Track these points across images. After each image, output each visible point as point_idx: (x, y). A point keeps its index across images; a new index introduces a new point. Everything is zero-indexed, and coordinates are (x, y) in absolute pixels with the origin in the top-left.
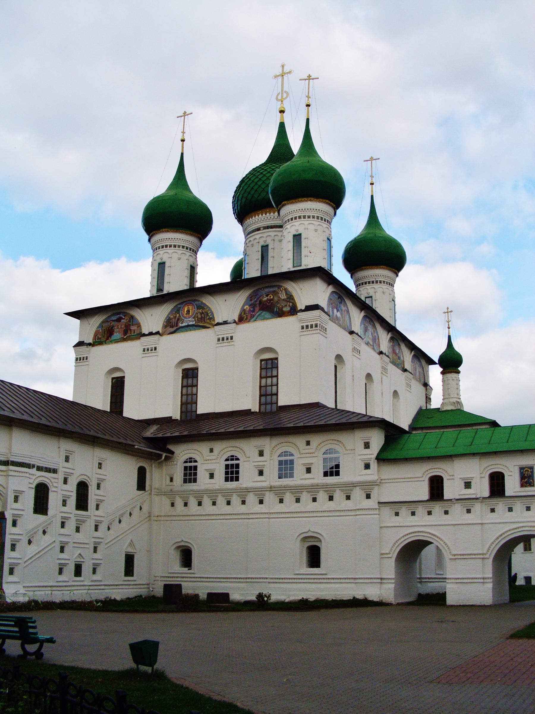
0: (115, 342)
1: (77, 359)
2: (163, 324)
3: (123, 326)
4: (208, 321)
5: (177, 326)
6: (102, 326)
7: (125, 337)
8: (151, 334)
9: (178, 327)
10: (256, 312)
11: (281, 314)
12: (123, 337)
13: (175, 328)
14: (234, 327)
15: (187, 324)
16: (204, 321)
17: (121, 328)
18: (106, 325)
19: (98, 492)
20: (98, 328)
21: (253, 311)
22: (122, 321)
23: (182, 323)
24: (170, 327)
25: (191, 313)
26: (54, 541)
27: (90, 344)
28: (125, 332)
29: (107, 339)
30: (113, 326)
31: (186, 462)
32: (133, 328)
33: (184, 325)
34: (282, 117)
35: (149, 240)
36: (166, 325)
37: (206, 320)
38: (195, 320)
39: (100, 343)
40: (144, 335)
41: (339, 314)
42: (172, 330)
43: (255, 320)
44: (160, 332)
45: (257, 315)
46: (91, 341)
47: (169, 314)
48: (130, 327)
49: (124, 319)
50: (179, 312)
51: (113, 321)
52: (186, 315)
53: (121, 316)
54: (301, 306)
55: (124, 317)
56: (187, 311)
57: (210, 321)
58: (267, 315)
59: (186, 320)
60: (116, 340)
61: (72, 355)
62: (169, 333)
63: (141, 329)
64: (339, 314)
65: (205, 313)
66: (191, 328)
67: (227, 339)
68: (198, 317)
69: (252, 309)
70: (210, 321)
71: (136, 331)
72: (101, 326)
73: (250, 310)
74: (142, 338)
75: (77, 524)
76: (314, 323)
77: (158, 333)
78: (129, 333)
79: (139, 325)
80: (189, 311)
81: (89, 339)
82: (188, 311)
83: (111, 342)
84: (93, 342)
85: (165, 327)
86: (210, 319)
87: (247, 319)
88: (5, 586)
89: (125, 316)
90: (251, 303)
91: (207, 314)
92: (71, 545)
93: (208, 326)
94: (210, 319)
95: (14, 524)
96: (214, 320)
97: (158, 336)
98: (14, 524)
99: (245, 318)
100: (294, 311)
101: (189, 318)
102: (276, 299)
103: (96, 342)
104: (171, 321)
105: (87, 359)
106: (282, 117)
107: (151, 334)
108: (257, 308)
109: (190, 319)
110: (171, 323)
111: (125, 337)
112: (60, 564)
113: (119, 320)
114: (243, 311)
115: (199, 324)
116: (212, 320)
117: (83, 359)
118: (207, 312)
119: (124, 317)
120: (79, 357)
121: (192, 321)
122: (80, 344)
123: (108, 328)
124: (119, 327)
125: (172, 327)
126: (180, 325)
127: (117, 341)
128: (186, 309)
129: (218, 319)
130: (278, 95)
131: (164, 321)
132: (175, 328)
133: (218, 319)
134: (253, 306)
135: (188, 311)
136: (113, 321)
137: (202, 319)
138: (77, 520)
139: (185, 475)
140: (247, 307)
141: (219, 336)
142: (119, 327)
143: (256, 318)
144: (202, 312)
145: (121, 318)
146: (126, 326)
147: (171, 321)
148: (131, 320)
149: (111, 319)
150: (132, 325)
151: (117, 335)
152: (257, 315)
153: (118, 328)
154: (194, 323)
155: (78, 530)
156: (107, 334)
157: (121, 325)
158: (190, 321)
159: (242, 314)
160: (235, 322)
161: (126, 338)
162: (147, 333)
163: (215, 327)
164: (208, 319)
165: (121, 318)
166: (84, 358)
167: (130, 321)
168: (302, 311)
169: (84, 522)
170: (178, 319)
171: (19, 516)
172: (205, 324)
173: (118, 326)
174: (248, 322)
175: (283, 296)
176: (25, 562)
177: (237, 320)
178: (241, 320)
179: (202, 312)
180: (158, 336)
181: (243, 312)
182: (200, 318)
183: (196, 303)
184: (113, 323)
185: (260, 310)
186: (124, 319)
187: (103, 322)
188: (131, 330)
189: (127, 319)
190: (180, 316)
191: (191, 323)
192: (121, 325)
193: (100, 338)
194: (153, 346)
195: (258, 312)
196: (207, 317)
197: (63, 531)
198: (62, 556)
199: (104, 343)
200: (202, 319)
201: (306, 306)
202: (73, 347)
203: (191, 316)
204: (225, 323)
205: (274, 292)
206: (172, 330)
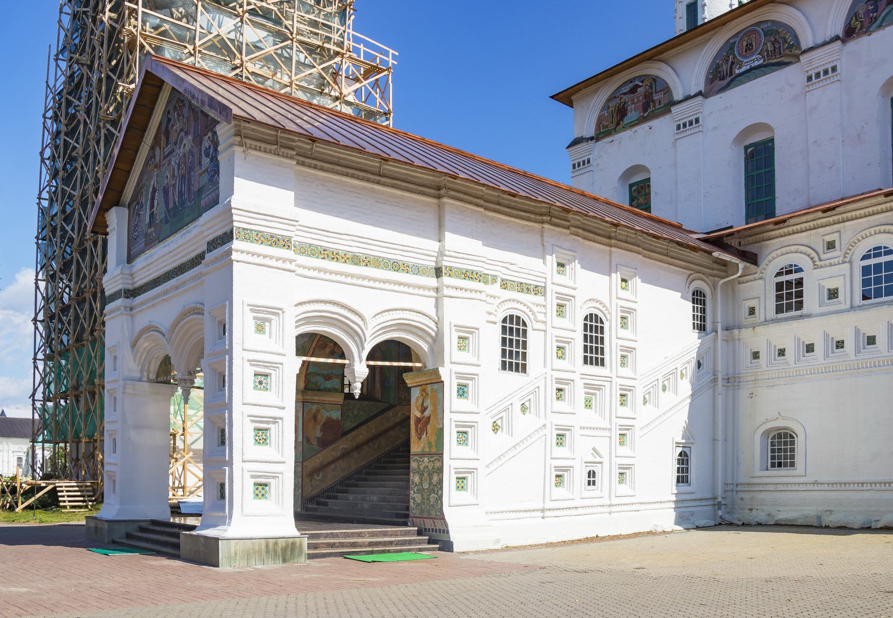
0: (630, 127)
2: (707, 77)
3: (641, 98)
4: (787, 52)
5: (731, 74)
6: (609, 107)
7: (646, 115)
8: (688, 98)
9: (734, 75)
10: (880, 10)
12: (643, 116)
13: (728, 79)
14: (838, 47)
15: (748, 67)
16: (780, 54)
17: (639, 101)
19: (623, 333)
20: (602, 110)
21: (876, 10)
22: (638, 90)
23: (740, 68)
24: (720, 80)
25: (754, 48)
26: (544, 425)
27: (592, 139)
28: (645, 108)
29: (618, 124)
30: (625, 103)
31: (779, 274)
33: (742, 70)
36: (711, 79)
37: (784, 51)
38: (763, 57)
39: (608, 134)
42: (725, 82)
43: (880, 27)
44: (703, 91)
45: (883, 14)
48: (652, 97)
49: (642, 86)
50: (734, 51)
51: (625, 94)
52: (746, 52)
53: (637, 82)
55: (641, 84)
56: (747, 46)
57: (791, 51)
59: (745, 61)
60: (631, 122)
62: (717, 90)
65: (780, 41)
66: (756, 71)
68: (767, 50)
69: (871, 8)
70: (791, 51)
71: (662, 102)
72: (606, 107)
74: (673, 109)
75: (586, 393)
77: (700, 93)
78: (651, 106)
79: (667, 90)
80: (751, 44)
81: (589, 130)
83: (623, 127)
84: (596, 134)
86: (790, 47)
87: (861, 28)
88: (446, 510)
89: (642, 82)
91: (785, 41)
92: (577, 431)
93: (786, 60)
94: (790, 47)
95: (462, 391)
97: (700, 98)
98: (462, 391)
99: (859, 27)
101: (752, 55)
103: (601, 133)
104: (720, 69)
105: (589, 161)
107: (688, 98)
109: (754, 57)
110: (720, 72)
111: (646, 115)
112: (557, 468)
113: (633, 90)
114: (853, 14)
115: (771, 61)
116: (794, 48)
117: (584, 164)
118: (784, 38)
119: (641, 84)
121: (758, 60)
123: (618, 107)
124: (635, 101)
125: (722, 79)
126: (737, 71)
127: (633, 125)
128: (745, 43)
129: (806, 41)
131: (708, 73)
132: (728, 79)
136: (625, 94)
137: (776, 52)
138: (587, 385)
141: (810, 73)
142: (635, 101)
143: (882, 22)
144: (775, 40)
145: (637, 86)
146: (646, 97)
147: (720, 69)
148: (654, 85)
149: (621, 92)
150: (656, 93)
151: (632, 115)
152: (883, 14)
153: (633, 103)
154: (761, 61)
155: (588, 405)
156: (617, 116)
157: (638, 98)
158: (754, 61)
159: (852, 22)
161: (648, 115)
162: (680, 98)
164: (787, 48)
165: (637, 86)
166: (584, 162)
167: (651, 87)
169: (599, 389)
170: (733, 63)
171: (472, 377)
172: (781, 59)
173: (633, 100)
174: (866, 32)
176: (487, 466)
178: (850, 33)
179: (775, 40)
180: (700, 99)
181: (854, 18)
182: (771, 51)
183: (762, 27)
184: (626, 98)
186: (642, 86)
187: (610, 100)
188: (654, 101)
189: (647, 85)
190: (735, 57)
191: (756, 63)
192: (638, 98)
193: (607, 127)
195: (883, 11)
196: (783, 44)
197: (559, 406)
198: (559, 452)
199: (613, 132)
200: (776, 52)
203: (756, 51)
206: (725, 82)
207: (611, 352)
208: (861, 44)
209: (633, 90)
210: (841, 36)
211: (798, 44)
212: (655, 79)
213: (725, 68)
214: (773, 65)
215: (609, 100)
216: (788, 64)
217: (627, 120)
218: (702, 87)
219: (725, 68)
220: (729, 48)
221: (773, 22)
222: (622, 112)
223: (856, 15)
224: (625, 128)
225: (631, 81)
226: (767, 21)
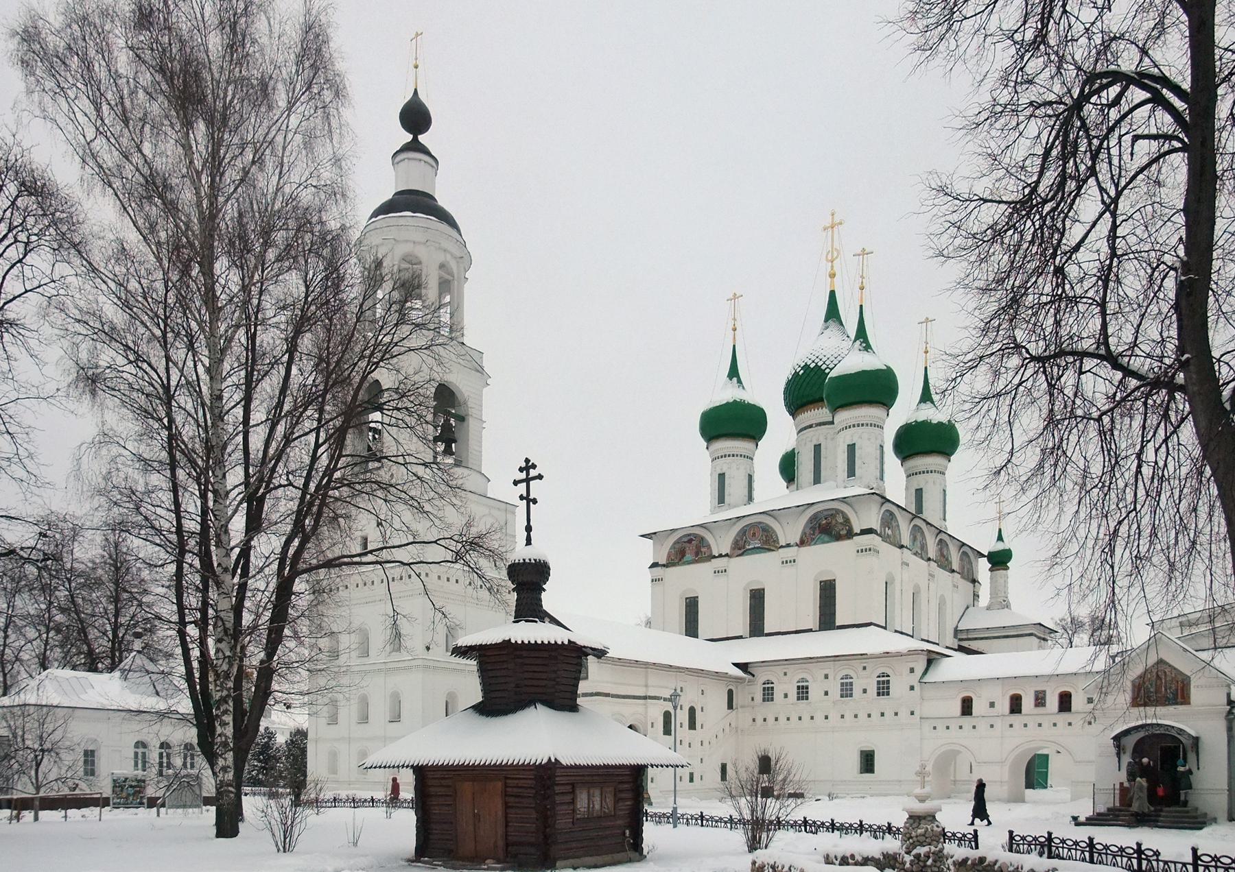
1: (652, 581)
8: (721, 556)
11: (838, 538)
18: (677, 546)
27: (664, 565)
28: (697, 554)
32: (703, 550)
33: (750, 547)
34: (832, 284)
35: (707, 448)
40: (715, 557)
41: (890, 532)
43: (815, 544)
46: (664, 562)
47: (738, 535)
54: (857, 530)
58: (826, 538)
61: (648, 575)
63: (711, 551)
64: (890, 532)
67: (790, 562)
73: (810, 533)
76: (868, 547)
77: (727, 555)
79: (709, 547)
82: (754, 534)
85: (733, 549)
86: (774, 541)
90: (811, 525)
96: (778, 543)
97: (727, 558)
100: (850, 535)
102: (834, 522)
106: (832, 284)
108: (817, 531)
113: (690, 541)
114: (804, 533)
120: (654, 578)
122: (655, 565)
125: (740, 549)
127: (689, 563)
129: (782, 543)
130: (827, 254)
132: (743, 550)
133: (782, 543)
134: (813, 528)
135: (754, 534)
137: (766, 542)
139: (764, 695)
140: (808, 531)
151: (688, 557)
160: (797, 545)
163: (780, 550)
168: (857, 534)
175: (840, 520)
177: (798, 543)
178: (802, 543)
185: (820, 533)
191: (757, 545)
194: (723, 569)
200: (766, 542)
201: (861, 530)
202: (650, 568)
204: (788, 545)
205: (832, 515)
206: (741, 552)
207: (698, 725)
208: (805, 550)
209: (690, 541)
210: (798, 543)
211: (777, 541)
212: (702, 539)
213: (741, 543)
214: (765, 549)
215: (675, 543)
216: (773, 550)
217: (685, 559)
218: (728, 551)
219: (741, 543)
220: (743, 532)
221: (767, 525)
222: (682, 553)
223: (805, 534)
224: (684, 564)
225: (689, 535)
226: (763, 523)
